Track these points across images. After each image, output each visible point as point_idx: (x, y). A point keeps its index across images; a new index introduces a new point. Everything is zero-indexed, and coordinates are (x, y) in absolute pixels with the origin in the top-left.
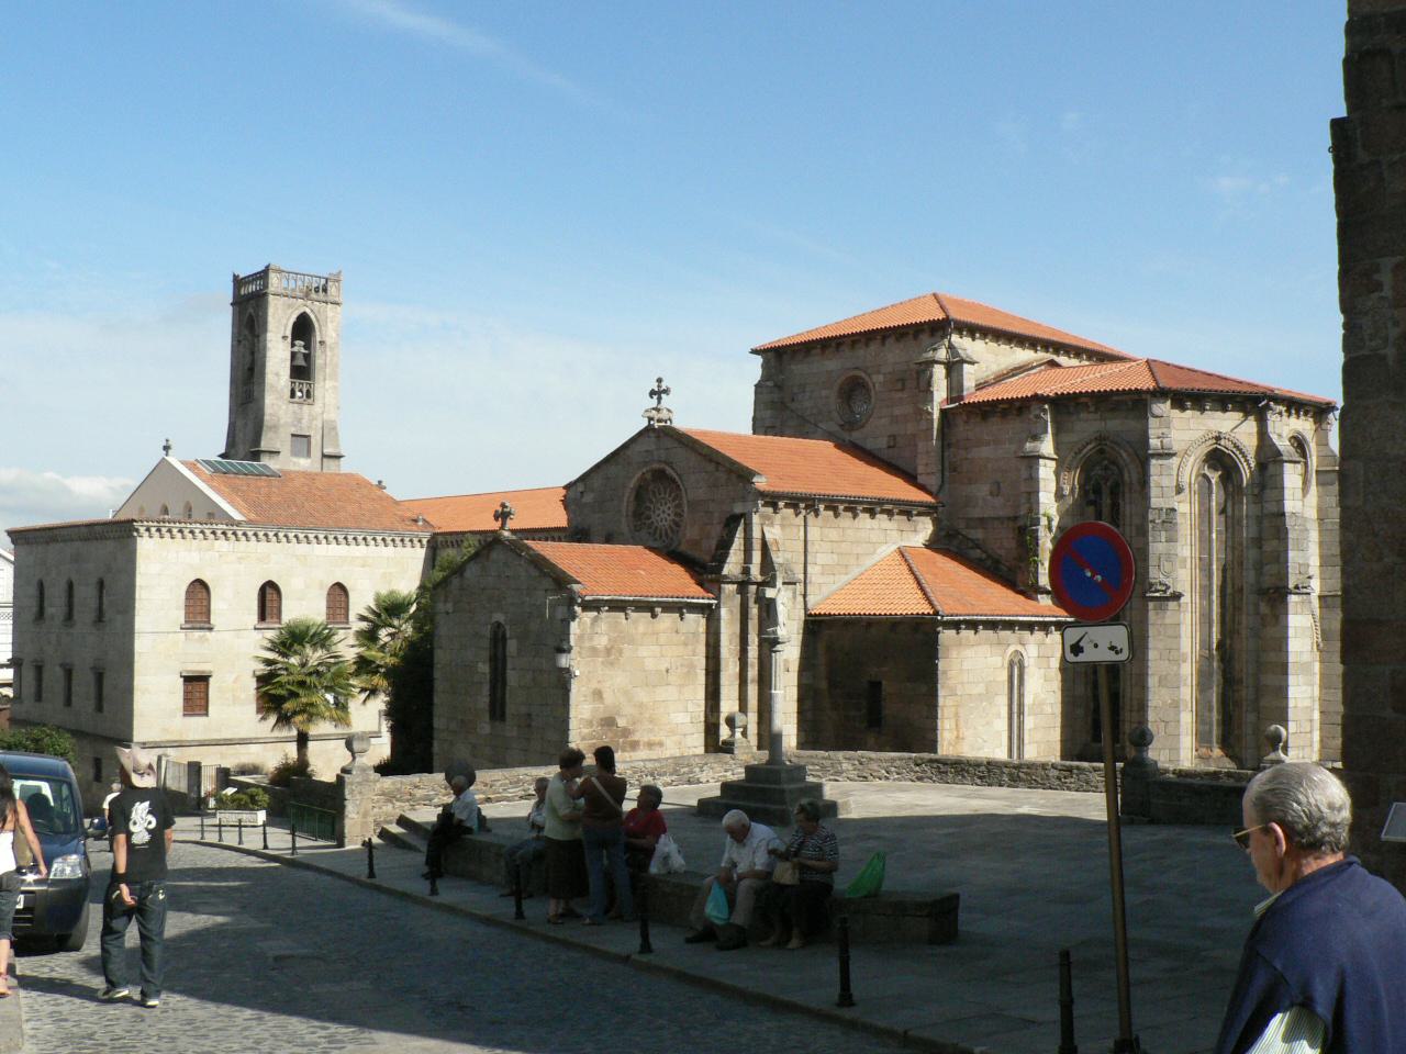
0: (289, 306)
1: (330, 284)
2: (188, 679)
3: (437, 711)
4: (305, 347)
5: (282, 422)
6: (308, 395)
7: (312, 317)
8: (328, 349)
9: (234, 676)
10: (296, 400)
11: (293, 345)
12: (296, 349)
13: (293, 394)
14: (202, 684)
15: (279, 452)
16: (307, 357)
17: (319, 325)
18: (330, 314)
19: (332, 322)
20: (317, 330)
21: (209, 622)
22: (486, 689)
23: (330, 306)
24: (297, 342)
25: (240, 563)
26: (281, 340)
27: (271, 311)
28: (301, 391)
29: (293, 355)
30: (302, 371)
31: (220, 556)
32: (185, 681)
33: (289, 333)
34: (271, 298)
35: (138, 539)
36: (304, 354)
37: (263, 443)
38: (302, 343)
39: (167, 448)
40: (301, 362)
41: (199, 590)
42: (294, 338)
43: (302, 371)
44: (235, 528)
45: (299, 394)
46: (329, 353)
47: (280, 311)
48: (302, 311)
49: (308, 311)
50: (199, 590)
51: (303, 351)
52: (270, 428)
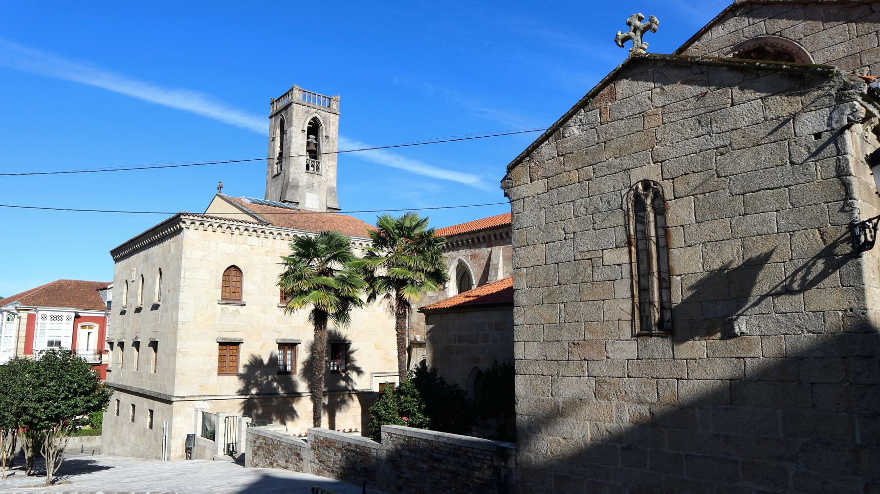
0: (307, 112)
1: (332, 102)
2: (221, 344)
3: (519, 334)
4: (316, 139)
5: (300, 184)
6: (318, 169)
7: (321, 120)
8: (330, 142)
9: (262, 343)
10: (310, 171)
11: (308, 138)
12: (310, 140)
13: (308, 168)
14: (235, 347)
15: (299, 203)
16: (316, 145)
17: (326, 126)
18: (332, 120)
19: (333, 125)
20: (324, 129)
21: (240, 300)
22: (623, 289)
23: (332, 115)
24: (311, 136)
25: (267, 256)
26: (300, 132)
27: (294, 113)
28: (313, 166)
29: (308, 143)
30: (313, 153)
31: (252, 249)
32: (219, 345)
33: (306, 129)
34: (294, 105)
35: (185, 230)
36: (316, 144)
37: (287, 198)
38: (314, 137)
39: (220, 188)
40: (313, 148)
41: (233, 273)
42: (308, 134)
43: (313, 153)
44: (264, 227)
45: (312, 168)
46: (331, 144)
47: (300, 115)
48: (314, 115)
49: (318, 116)
50: (233, 273)
51: (315, 142)
52: (293, 187)
